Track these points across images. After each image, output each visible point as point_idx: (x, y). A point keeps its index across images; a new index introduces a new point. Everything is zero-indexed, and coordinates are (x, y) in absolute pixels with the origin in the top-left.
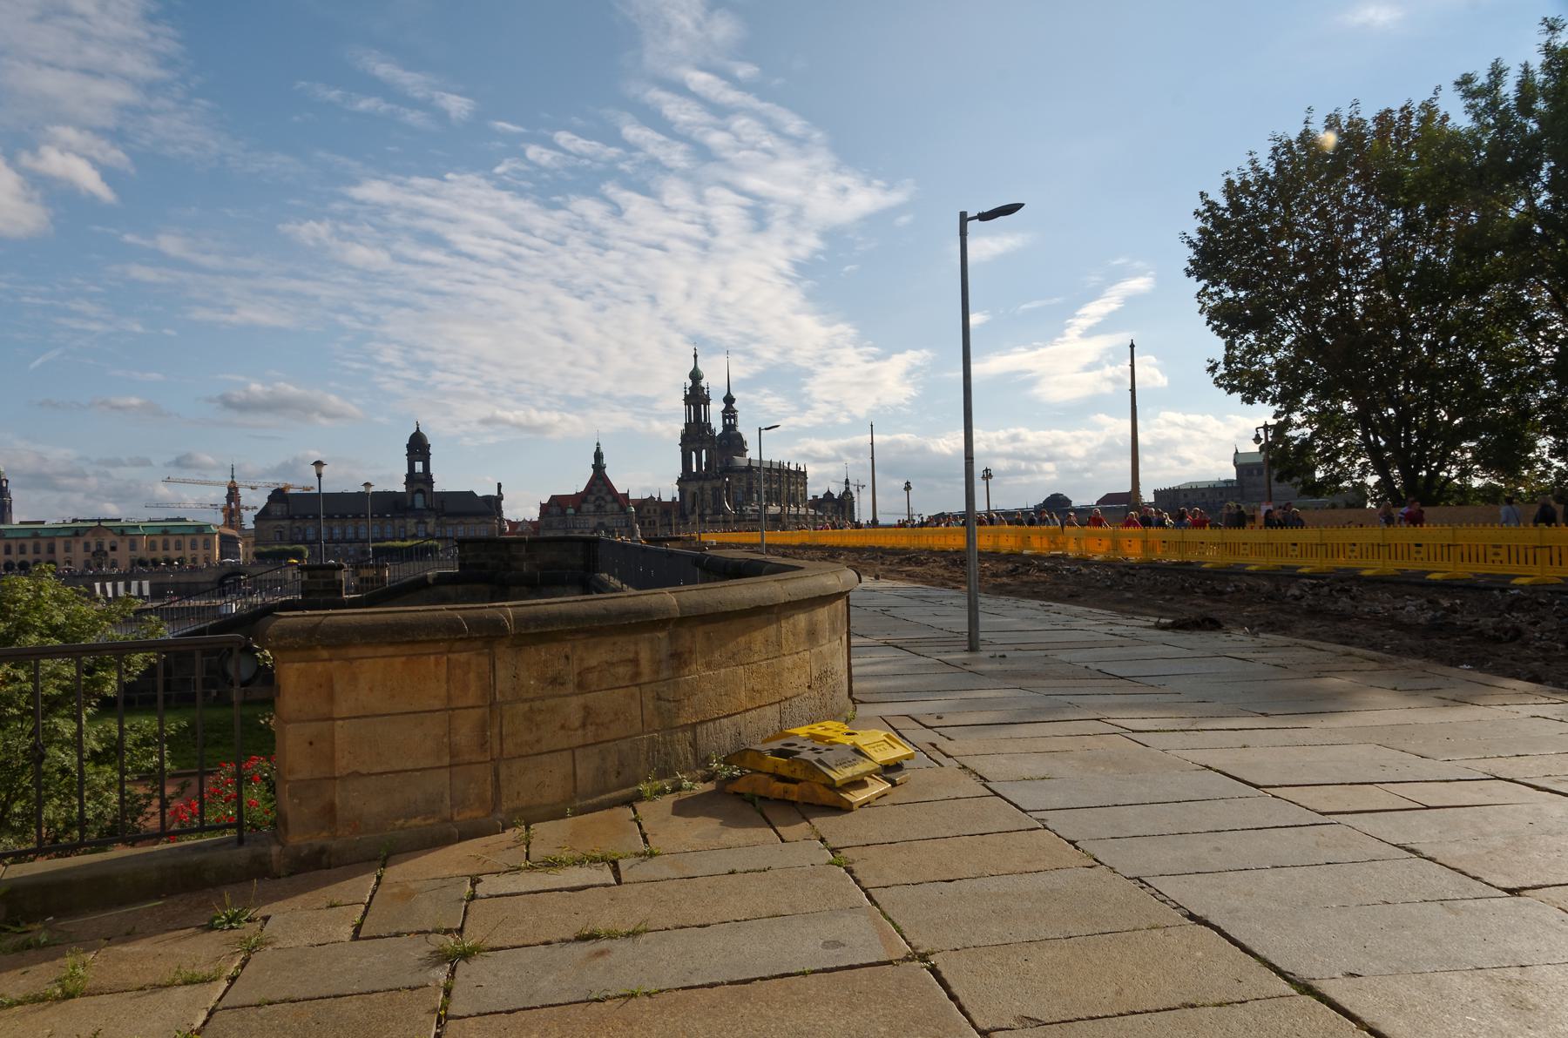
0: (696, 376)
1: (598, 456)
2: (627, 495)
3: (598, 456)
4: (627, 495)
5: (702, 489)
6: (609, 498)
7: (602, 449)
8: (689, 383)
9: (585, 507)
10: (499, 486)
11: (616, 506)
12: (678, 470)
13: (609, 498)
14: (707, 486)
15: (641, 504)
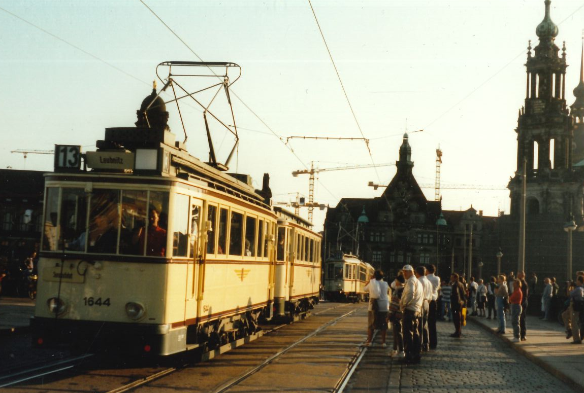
0: (546, 32)
1: (405, 151)
2: (438, 204)
3: (405, 151)
4: (438, 204)
5: (547, 195)
6: (415, 206)
7: (411, 143)
8: (536, 42)
9: (382, 217)
10: (266, 178)
11: (422, 216)
12: (510, 168)
13: (415, 206)
14: (556, 190)
15: (456, 217)
